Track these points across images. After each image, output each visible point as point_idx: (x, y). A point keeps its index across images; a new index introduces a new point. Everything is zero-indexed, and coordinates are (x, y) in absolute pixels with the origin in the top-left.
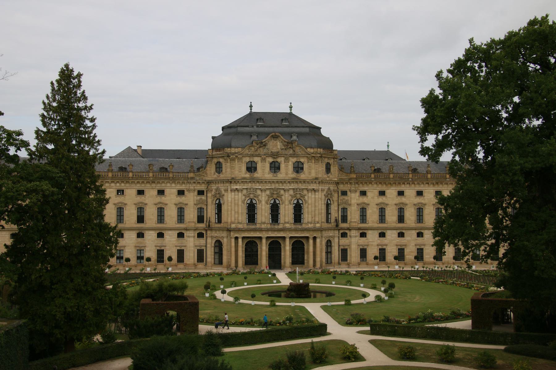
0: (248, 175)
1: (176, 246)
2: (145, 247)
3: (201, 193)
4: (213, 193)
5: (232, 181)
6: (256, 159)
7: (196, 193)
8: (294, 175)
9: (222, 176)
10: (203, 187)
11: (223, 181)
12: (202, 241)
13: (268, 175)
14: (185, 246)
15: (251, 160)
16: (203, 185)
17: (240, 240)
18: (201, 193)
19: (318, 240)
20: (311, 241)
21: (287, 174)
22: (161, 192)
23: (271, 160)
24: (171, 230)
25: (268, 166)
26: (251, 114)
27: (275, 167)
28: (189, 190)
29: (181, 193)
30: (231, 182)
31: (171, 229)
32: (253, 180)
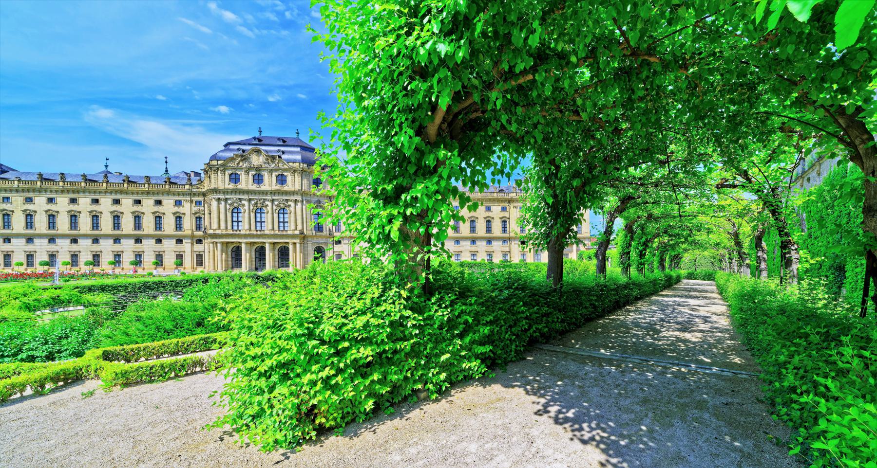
0: (231, 186)
3: (198, 203)
5: (216, 191)
7: (194, 204)
8: (278, 187)
10: (201, 199)
15: (234, 171)
17: (219, 245)
18: (198, 203)
19: (298, 246)
20: (291, 247)
21: (270, 185)
22: (159, 203)
23: (254, 173)
25: (251, 178)
27: (258, 179)
28: (186, 201)
29: (178, 203)
32: (235, 191)
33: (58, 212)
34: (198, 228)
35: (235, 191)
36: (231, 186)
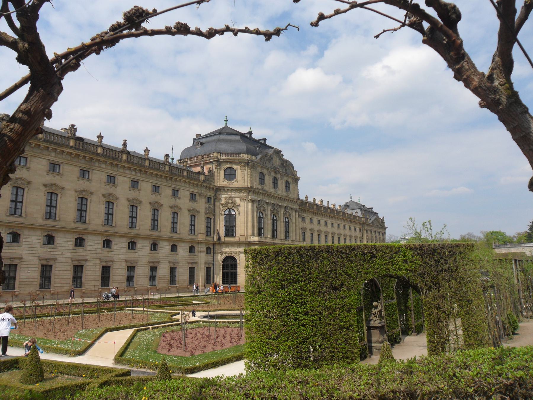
0: (260, 187)
1: (188, 263)
2: (159, 263)
4: (223, 201)
6: (265, 171)
9: (235, 184)
10: (211, 194)
11: (239, 190)
12: (210, 258)
13: (272, 190)
14: (196, 263)
16: (212, 192)
24: (184, 242)
26: (226, 128)
27: (275, 182)
28: (200, 195)
30: (250, 191)
31: (184, 242)
33: (62, 189)
34: (208, 233)
35: (266, 194)
36: (260, 187)
